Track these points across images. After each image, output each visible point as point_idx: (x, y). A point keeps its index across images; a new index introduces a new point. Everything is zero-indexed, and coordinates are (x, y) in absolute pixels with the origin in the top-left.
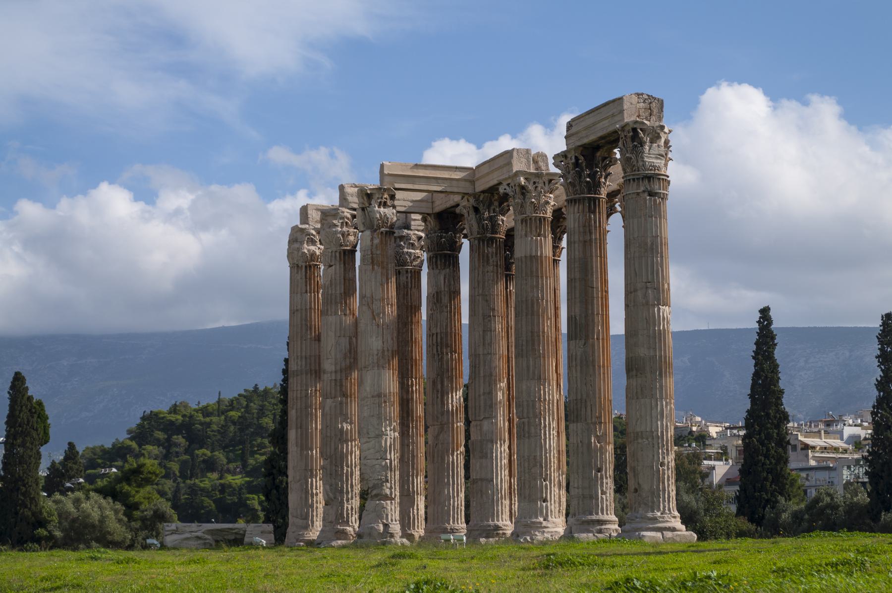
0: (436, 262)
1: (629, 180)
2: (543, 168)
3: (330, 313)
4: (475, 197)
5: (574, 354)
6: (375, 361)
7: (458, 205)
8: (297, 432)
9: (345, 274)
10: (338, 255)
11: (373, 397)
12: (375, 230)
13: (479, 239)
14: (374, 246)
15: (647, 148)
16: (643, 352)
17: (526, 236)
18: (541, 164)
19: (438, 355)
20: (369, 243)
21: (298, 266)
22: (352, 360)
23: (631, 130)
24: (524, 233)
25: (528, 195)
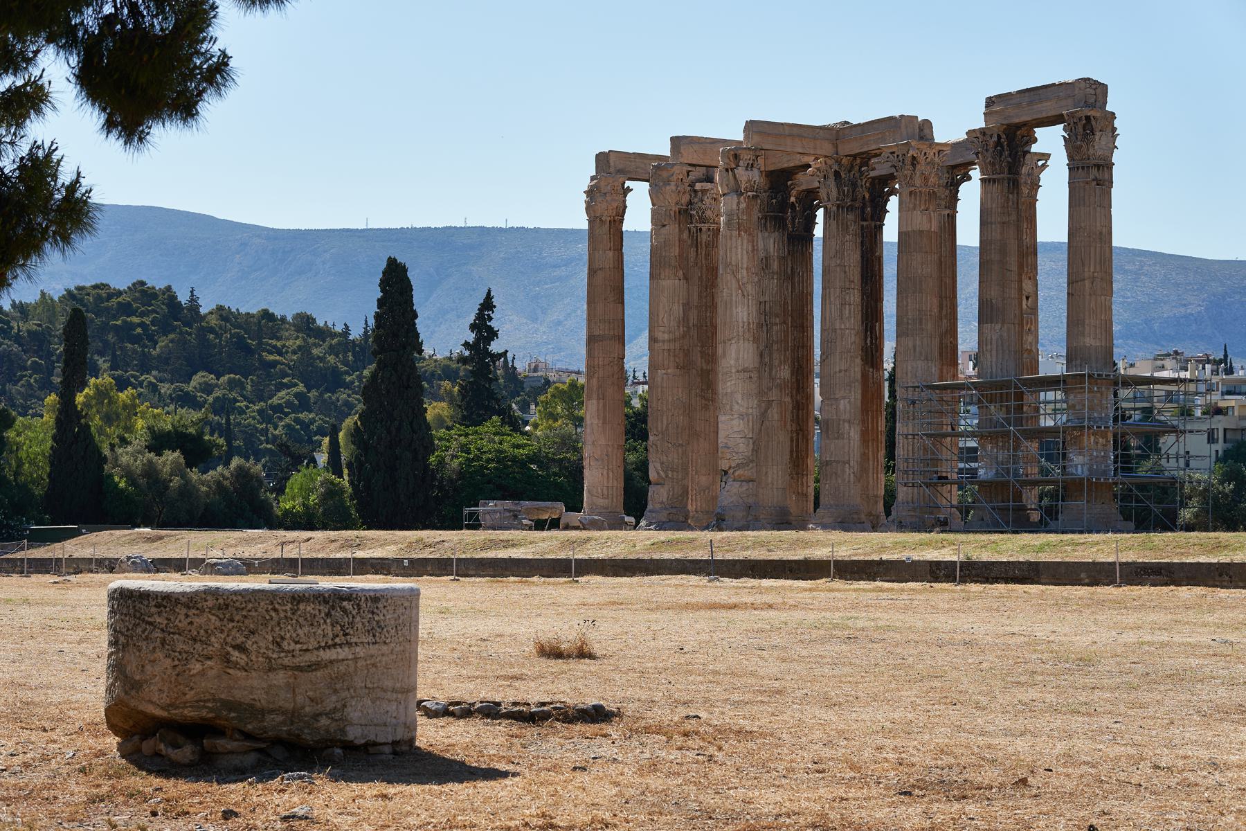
0: (765, 224)
1: (1078, 168)
2: (928, 137)
3: (662, 277)
4: (837, 161)
5: (989, 338)
6: (741, 334)
7: (810, 166)
8: (598, 403)
9: (680, 235)
10: (672, 214)
11: (738, 372)
12: (742, 194)
13: (838, 206)
14: (741, 211)
15: (1097, 138)
16: (1089, 341)
17: (914, 209)
18: (926, 131)
19: (767, 325)
20: (735, 207)
21: (601, 220)
22: (685, 329)
23: (1084, 118)
24: (911, 206)
25: (918, 167)
